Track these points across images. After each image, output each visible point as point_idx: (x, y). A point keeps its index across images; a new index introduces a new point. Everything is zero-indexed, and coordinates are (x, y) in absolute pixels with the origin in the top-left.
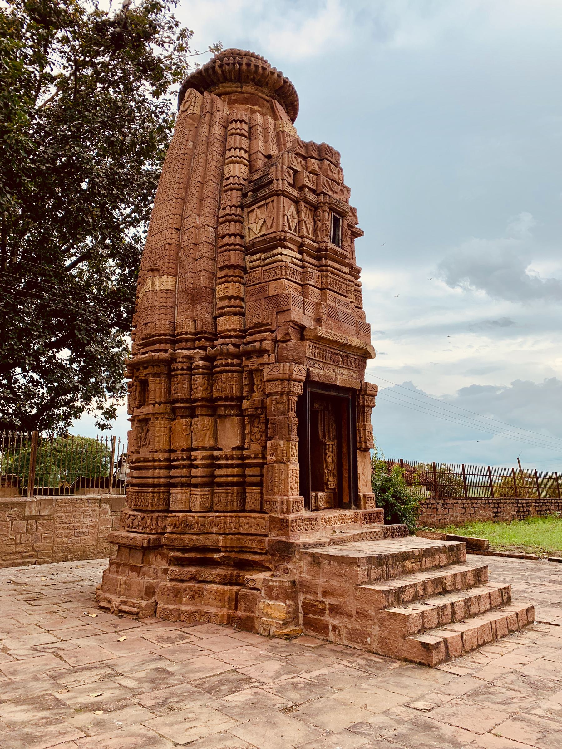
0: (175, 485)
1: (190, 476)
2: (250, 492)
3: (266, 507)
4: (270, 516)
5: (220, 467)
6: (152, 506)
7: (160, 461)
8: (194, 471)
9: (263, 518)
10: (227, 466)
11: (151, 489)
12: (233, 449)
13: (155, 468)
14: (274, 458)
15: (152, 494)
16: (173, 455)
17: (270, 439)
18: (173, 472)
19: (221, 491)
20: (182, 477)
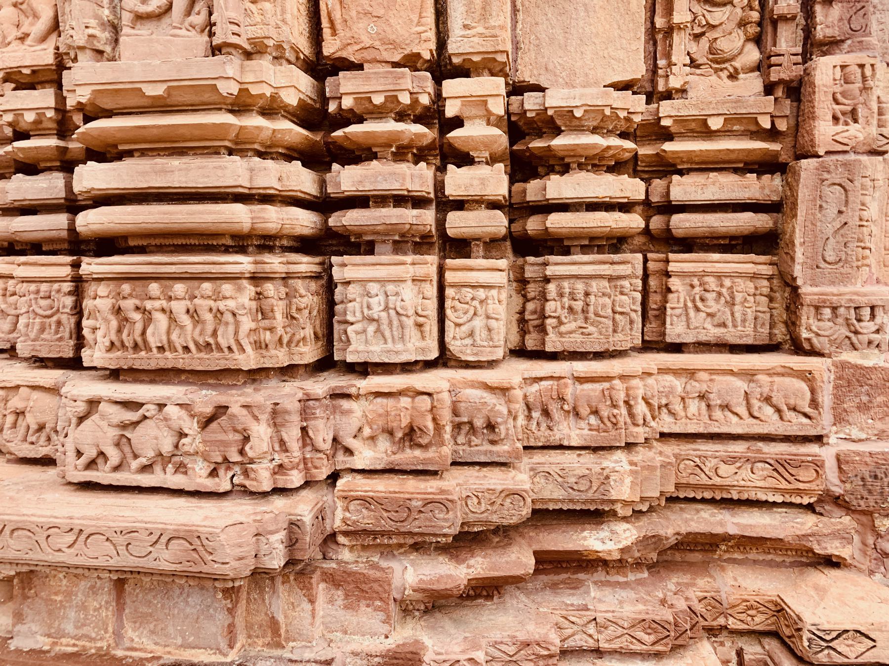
0: (359, 244)
1: (447, 205)
2: (682, 275)
3: (810, 327)
4: (843, 365)
5: (561, 165)
6: (260, 346)
7: (270, 109)
8: (459, 181)
10: (597, 163)
11: (243, 263)
13: (239, 147)
14: (855, 132)
15: (250, 290)
16: (347, 89)
17: (831, 45)
18: (347, 179)
20: (400, 200)
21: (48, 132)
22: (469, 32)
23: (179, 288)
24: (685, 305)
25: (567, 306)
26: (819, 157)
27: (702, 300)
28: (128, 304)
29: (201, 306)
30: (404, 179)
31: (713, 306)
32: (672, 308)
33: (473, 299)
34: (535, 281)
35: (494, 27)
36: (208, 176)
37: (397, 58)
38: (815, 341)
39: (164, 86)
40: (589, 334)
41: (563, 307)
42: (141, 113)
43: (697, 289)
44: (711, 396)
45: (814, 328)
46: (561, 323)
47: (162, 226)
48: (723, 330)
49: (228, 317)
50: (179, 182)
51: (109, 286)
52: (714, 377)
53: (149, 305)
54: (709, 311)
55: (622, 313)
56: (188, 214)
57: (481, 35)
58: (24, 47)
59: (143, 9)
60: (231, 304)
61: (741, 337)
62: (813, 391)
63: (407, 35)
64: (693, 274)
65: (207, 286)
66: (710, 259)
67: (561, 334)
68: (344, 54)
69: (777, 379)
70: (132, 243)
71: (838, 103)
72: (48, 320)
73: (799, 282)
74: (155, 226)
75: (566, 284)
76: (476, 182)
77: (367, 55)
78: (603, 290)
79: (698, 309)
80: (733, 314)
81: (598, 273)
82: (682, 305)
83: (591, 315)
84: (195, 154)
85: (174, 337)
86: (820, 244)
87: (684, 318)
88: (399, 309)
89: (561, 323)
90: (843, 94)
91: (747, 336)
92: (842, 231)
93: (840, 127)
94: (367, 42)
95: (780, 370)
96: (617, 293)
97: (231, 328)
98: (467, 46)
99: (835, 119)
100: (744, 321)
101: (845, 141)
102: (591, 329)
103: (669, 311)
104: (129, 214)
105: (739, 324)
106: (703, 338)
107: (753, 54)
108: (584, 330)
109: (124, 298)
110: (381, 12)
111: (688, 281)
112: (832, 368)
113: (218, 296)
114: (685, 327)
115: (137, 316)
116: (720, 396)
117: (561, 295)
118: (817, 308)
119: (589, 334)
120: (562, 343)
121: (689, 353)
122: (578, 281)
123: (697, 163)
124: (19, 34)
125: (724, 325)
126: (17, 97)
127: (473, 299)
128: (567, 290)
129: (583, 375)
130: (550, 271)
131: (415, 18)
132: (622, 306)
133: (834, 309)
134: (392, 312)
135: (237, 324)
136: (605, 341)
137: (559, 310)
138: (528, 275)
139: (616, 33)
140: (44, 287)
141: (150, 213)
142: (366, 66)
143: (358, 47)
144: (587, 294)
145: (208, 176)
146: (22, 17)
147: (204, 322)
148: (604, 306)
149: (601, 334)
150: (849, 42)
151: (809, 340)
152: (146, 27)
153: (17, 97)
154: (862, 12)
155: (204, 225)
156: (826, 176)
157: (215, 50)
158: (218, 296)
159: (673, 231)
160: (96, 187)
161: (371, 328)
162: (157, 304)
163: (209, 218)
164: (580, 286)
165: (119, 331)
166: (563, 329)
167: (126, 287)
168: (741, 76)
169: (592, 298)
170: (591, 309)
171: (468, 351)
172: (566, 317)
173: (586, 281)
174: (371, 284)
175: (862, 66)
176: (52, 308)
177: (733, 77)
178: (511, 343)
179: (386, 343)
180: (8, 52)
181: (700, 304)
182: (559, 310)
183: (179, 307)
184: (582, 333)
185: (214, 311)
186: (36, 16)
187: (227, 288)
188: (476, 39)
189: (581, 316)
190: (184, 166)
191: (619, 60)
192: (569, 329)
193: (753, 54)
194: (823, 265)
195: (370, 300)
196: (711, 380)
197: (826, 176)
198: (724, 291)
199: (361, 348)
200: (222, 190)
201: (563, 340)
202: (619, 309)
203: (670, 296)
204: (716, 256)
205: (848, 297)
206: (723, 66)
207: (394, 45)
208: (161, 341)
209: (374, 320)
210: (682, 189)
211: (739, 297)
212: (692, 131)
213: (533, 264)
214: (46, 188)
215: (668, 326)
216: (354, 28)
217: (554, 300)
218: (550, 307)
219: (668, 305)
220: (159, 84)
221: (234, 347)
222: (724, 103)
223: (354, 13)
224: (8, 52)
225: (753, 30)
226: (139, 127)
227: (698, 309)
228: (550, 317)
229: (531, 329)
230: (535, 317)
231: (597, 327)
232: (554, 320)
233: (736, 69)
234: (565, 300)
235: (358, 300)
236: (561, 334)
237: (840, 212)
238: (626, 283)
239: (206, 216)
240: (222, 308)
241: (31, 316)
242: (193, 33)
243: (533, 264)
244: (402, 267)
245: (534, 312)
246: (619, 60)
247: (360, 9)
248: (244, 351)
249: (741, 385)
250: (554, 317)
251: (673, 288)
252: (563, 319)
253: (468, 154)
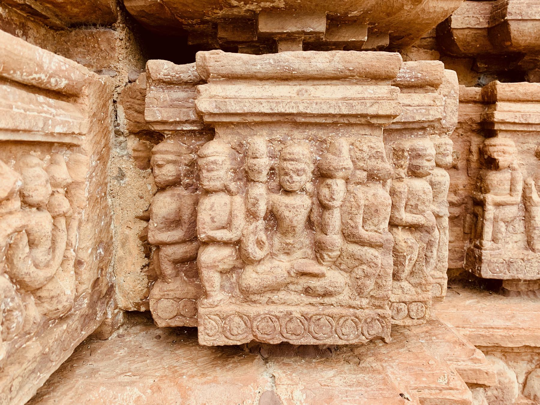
2: (523, 129)
25: (262, 209)
32: (498, 205)
34: (177, 134)
40: (327, 294)
41: (251, 215)
46: (244, 260)
55: (413, 228)
67: (247, 295)
75: (260, 142)
78: (372, 163)
81: (359, 109)
82: (518, 198)
83: (334, 238)
87: (520, 226)
89: (244, 260)
96: (403, 172)
102: (334, 278)
103: (491, 211)
108: (313, 283)
114: (522, 244)
117: (247, 177)
119: (327, 294)
120: (247, 320)
122: (297, 134)
128: (264, 163)
130: (211, 99)
132: (413, 209)
136: (370, 312)
137: (240, 221)
138: (154, 113)
144: (322, 175)
148: (371, 212)
149: (360, 291)
159: (514, 27)
164: (302, 150)
166: (251, 277)
169: (338, 186)
170: (335, 219)
172: (260, 244)
173: (321, 134)
178: (125, 295)
182: (240, 221)
184: (307, 291)
189: (303, 239)
192: (269, 279)
201: (252, 310)
202: (407, 217)
203: (494, 177)
213: (169, 83)
215: (487, 242)
217: (226, 190)
218: (213, 211)
219: (490, 198)
228: (211, 242)
229: (168, 269)
230: (177, 234)
231: (350, 271)
232: (227, 252)
234: (259, 191)
236: (247, 295)
238: (427, 144)
243: (169, 83)
245: (175, 222)
250: (226, 244)
251: (502, 160)
252: (253, 250)
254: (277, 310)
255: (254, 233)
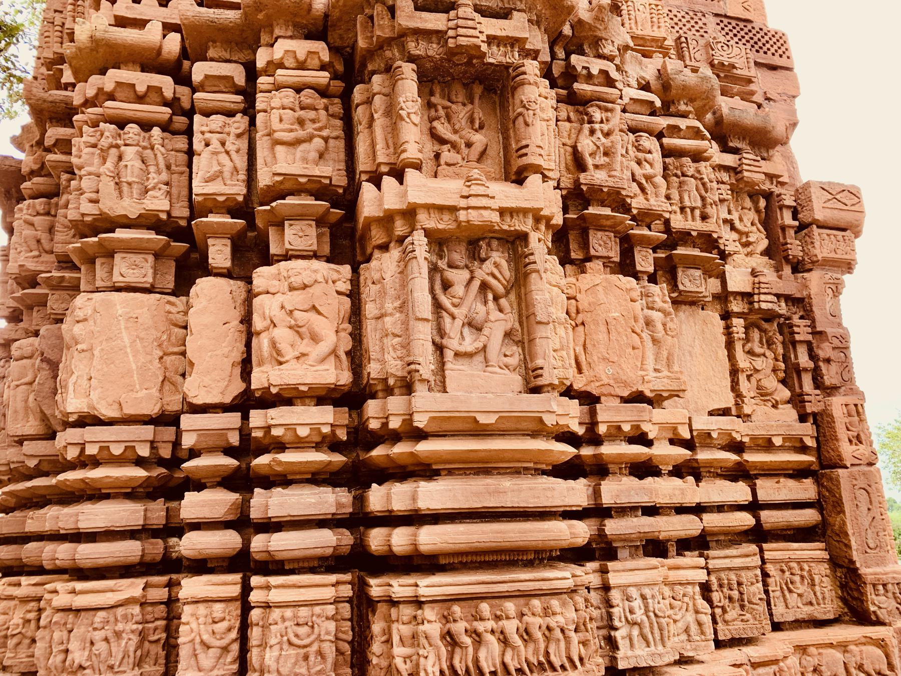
9: (881, 644)
12: (711, 414)
19: (738, 562)
21: (302, 445)
22: (658, 374)
23: (510, 606)
24: (781, 588)
26: (847, 468)
27: (792, 583)
28: (459, 627)
29: (533, 624)
30: (651, 493)
31: (802, 588)
33: (684, 595)
35: (677, 372)
36: (539, 497)
37: (626, 394)
38: (878, 612)
39: (496, 416)
41: (725, 597)
42: (452, 435)
43: (787, 574)
44: (823, 668)
45: (876, 603)
47: (494, 544)
48: (812, 608)
49: (558, 634)
50: (512, 502)
51: (433, 608)
52: (821, 651)
53: (480, 626)
54: (799, 592)
56: (520, 532)
57: (668, 377)
58: (305, 366)
59: (462, 349)
60: (560, 619)
61: (825, 613)
62: (887, 656)
63: (634, 377)
64: (781, 561)
65: (536, 603)
66: (791, 548)
68: (588, 389)
69: (863, 648)
70: (443, 561)
71: (848, 430)
72: (302, 651)
73: (858, 565)
74: (487, 544)
75: (723, 575)
76: (677, 492)
77: (605, 390)
79: (790, 591)
80: (815, 594)
82: (779, 588)
84: (499, 474)
85: (508, 659)
86: (863, 534)
87: (782, 599)
88: (657, 611)
90: (850, 423)
91: (829, 611)
92: (873, 524)
93: (854, 447)
94: (606, 381)
95: (864, 640)
97: (563, 644)
98: (660, 385)
99: (850, 441)
100: (824, 598)
101: (859, 457)
102: (748, 616)
104: (463, 533)
105: (821, 602)
106: (800, 616)
107: (786, 394)
109: (455, 621)
110: (616, 359)
111: (778, 566)
112: (895, 635)
113: (547, 612)
115: (467, 640)
116: (829, 668)
118: (874, 585)
121: (787, 630)
123: (763, 470)
124: (297, 354)
125: (811, 604)
126: (293, 412)
127: (684, 595)
129: (758, 660)
131: (639, 364)
133: (884, 585)
134: (652, 614)
135: (567, 639)
137: (722, 600)
139: (712, 373)
140: (304, 612)
141: (483, 533)
142: (603, 399)
143: (597, 384)
144: (739, 584)
145: (539, 497)
146: (297, 338)
147: (535, 641)
150: (843, 388)
151: (874, 612)
152: (460, 363)
153: (293, 412)
154: (847, 369)
155: (534, 543)
156: (855, 482)
157: (536, 390)
158: (547, 612)
160: (431, 508)
161: (636, 632)
162: (490, 624)
163: (540, 536)
165: (451, 658)
167: (456, 609)
168: (780, 406)
171: (689, 647)
174: (631, 588)
175: (856, 405)
176: (309, 636)
177: (775, 406)
179: (648, 646)
180: (287, 370)
181: (790, 586)
182: (722, 600)
183: (511, 626)
184: (742, 620)
185: (544, 628)
186: (315, 338)
187: (555, 603)
188: (665, 380)
190: (516, 487)
191: (716, 393)
193: (786, 394)
194: (868, 550)
195: (631, 604)
196: (819, 654)
197: (855, 482)
198: (805, 573)
199: (630, 653)
200: (548, 510)
204: (795, 545)
205: (891, 575)
206: (768, 398)
207: (626, 384)
208: (495, 666)
209: (635, 624)
210: (768, 490)
211: (817, 578)
212: (758, 445)
214: (314, 504)
216: (596, 369)
219: (770, 588)
220: (492, 414)
221: (567, 665)
222: (781, 426)
223: (595, 358)
224: (287, 370)
225: (782, 375)
226: (471, 451)
227: (790, 591)
231: (751, 613)
233: (777, 401)
234: (725, 590)
235: (621, 605)
237: (869, 509)
239: (536, 534)
240: (553, 624)
241: (285, 646)
242: (507, 371)
244: (655, 571)
246: (716, 393)
247: (600, 355)
248: (575, 667)
249: (838, 655)
251: (771, 573)
253: (657, 466)
254: (736, 627)
255: (726, 602)
